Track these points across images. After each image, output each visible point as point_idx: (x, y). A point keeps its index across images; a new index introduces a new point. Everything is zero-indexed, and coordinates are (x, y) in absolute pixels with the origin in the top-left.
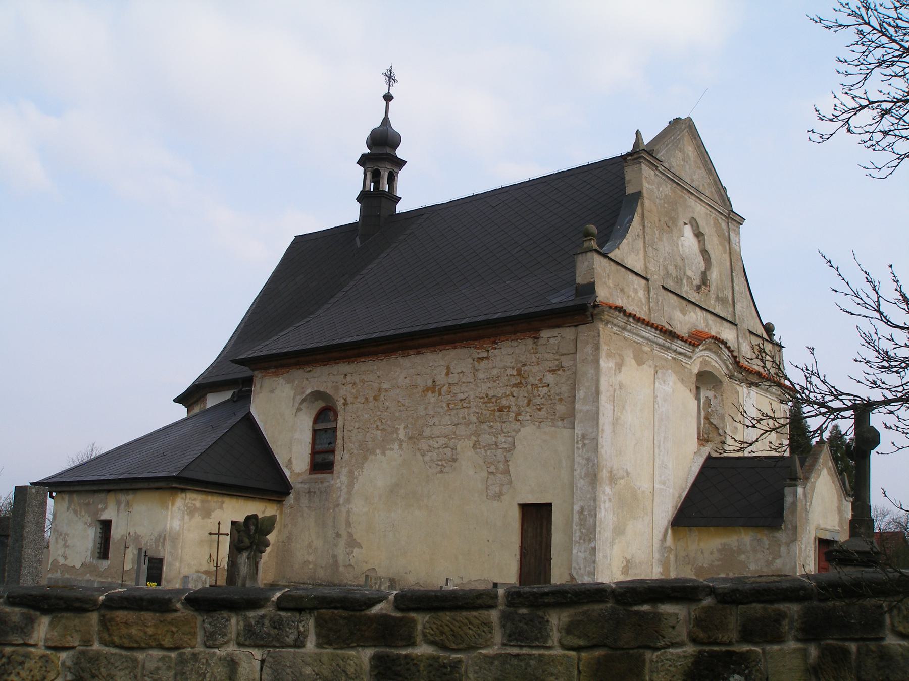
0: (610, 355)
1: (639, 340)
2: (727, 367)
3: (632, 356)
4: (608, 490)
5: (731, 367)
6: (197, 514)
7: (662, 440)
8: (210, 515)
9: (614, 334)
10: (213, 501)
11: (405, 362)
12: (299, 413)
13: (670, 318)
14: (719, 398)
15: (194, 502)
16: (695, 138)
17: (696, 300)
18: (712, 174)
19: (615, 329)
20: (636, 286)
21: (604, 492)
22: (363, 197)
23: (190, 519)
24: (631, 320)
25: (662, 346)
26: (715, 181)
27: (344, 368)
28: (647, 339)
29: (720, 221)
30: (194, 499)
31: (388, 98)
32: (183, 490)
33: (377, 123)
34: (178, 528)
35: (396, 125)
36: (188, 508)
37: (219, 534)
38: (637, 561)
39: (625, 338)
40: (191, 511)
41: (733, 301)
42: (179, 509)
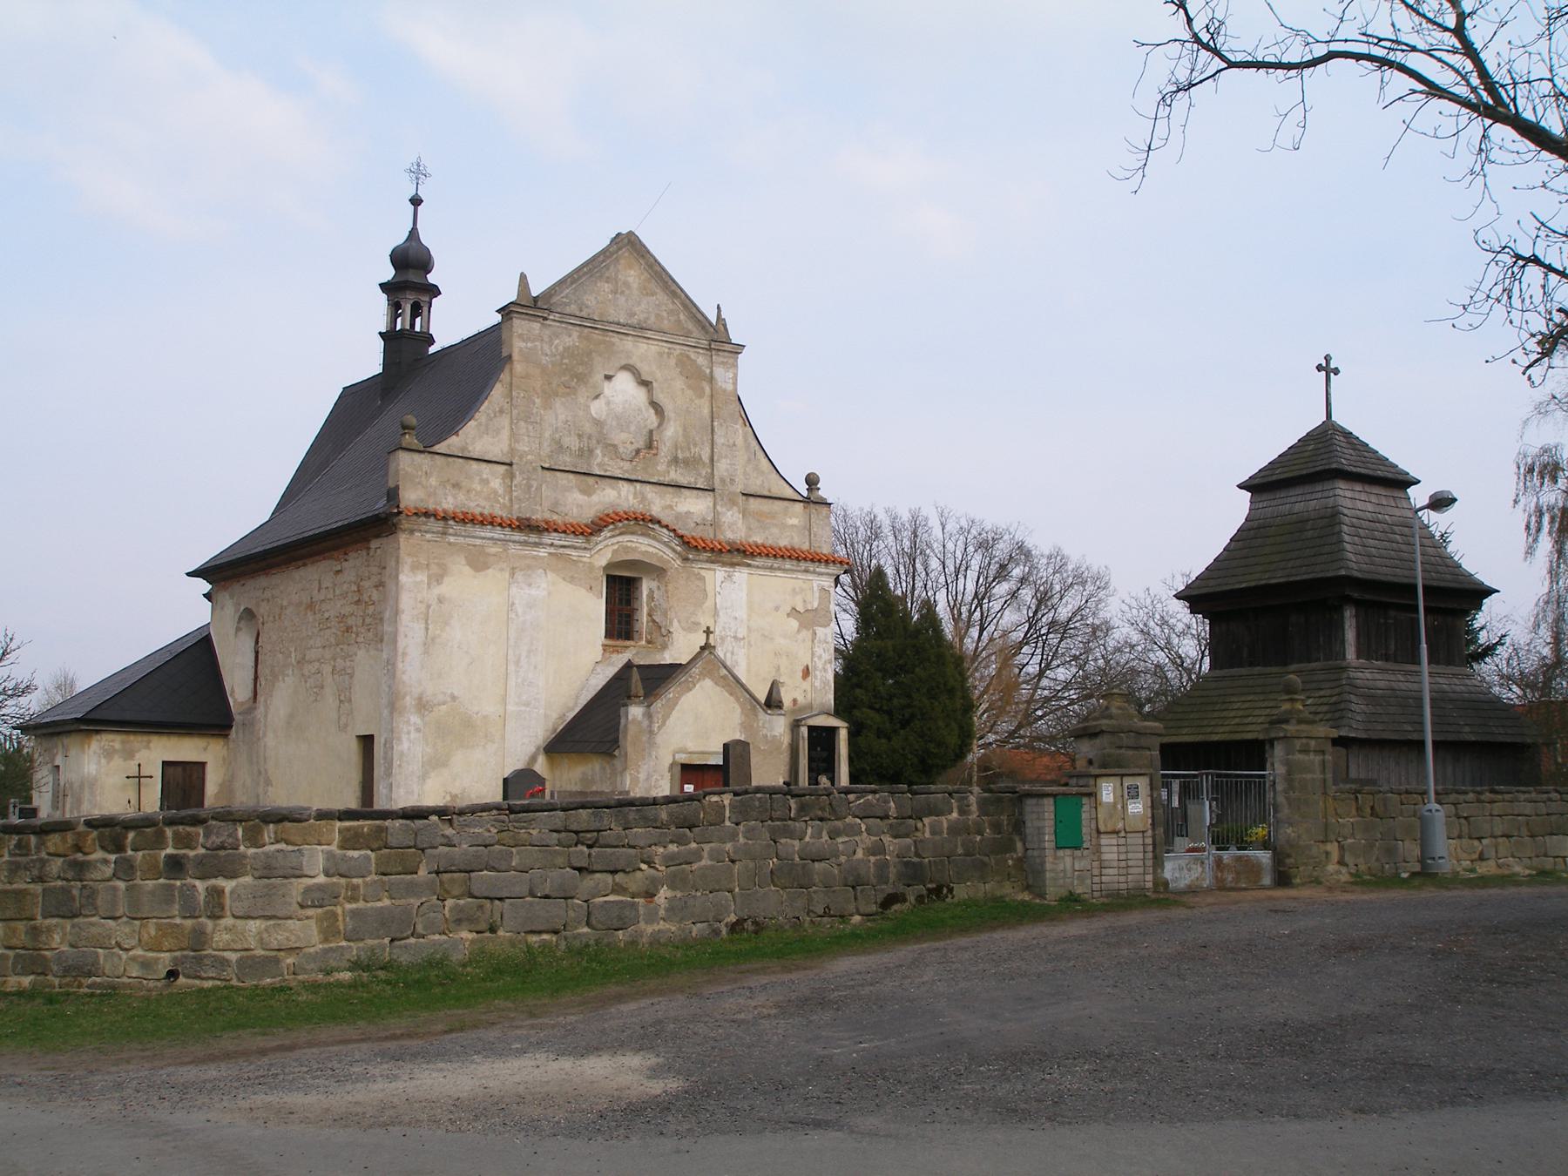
0: (415, 568)
1: (478, 542)
2: (674, 550)
3: (464, 562)
4: (415, 719)
5: (679, 549)
6: (116, 757)
7: (524, 654)
8: (134, 756)
9: (429, 541)
10: (136, 741)
11: (302, 572)
12: (240, 633)
13: (556, 503)
14: (663, 589)
16: (643, 256)
17: (627, 471)
18: (679, 297)
19: (428, 536)
20: (485, 476)
21: (408, 722)
22: (389, 337)
23: (108, 763)
24: (451, 522)
25: (525, 543)
26: (685, 306)
27: (263, 581)
28: (491, 539)
29: (693, 356)
30: (113, 741)
31: (416, 202)
32: (98, 732)
33: (400, 238)
34: (94, 772)
35: (426, 239)
36: (104, 750)
37: (139, 777)
39: (450, 544)
40: (109, 754)
41: (712, 460)
42: (95, 753)
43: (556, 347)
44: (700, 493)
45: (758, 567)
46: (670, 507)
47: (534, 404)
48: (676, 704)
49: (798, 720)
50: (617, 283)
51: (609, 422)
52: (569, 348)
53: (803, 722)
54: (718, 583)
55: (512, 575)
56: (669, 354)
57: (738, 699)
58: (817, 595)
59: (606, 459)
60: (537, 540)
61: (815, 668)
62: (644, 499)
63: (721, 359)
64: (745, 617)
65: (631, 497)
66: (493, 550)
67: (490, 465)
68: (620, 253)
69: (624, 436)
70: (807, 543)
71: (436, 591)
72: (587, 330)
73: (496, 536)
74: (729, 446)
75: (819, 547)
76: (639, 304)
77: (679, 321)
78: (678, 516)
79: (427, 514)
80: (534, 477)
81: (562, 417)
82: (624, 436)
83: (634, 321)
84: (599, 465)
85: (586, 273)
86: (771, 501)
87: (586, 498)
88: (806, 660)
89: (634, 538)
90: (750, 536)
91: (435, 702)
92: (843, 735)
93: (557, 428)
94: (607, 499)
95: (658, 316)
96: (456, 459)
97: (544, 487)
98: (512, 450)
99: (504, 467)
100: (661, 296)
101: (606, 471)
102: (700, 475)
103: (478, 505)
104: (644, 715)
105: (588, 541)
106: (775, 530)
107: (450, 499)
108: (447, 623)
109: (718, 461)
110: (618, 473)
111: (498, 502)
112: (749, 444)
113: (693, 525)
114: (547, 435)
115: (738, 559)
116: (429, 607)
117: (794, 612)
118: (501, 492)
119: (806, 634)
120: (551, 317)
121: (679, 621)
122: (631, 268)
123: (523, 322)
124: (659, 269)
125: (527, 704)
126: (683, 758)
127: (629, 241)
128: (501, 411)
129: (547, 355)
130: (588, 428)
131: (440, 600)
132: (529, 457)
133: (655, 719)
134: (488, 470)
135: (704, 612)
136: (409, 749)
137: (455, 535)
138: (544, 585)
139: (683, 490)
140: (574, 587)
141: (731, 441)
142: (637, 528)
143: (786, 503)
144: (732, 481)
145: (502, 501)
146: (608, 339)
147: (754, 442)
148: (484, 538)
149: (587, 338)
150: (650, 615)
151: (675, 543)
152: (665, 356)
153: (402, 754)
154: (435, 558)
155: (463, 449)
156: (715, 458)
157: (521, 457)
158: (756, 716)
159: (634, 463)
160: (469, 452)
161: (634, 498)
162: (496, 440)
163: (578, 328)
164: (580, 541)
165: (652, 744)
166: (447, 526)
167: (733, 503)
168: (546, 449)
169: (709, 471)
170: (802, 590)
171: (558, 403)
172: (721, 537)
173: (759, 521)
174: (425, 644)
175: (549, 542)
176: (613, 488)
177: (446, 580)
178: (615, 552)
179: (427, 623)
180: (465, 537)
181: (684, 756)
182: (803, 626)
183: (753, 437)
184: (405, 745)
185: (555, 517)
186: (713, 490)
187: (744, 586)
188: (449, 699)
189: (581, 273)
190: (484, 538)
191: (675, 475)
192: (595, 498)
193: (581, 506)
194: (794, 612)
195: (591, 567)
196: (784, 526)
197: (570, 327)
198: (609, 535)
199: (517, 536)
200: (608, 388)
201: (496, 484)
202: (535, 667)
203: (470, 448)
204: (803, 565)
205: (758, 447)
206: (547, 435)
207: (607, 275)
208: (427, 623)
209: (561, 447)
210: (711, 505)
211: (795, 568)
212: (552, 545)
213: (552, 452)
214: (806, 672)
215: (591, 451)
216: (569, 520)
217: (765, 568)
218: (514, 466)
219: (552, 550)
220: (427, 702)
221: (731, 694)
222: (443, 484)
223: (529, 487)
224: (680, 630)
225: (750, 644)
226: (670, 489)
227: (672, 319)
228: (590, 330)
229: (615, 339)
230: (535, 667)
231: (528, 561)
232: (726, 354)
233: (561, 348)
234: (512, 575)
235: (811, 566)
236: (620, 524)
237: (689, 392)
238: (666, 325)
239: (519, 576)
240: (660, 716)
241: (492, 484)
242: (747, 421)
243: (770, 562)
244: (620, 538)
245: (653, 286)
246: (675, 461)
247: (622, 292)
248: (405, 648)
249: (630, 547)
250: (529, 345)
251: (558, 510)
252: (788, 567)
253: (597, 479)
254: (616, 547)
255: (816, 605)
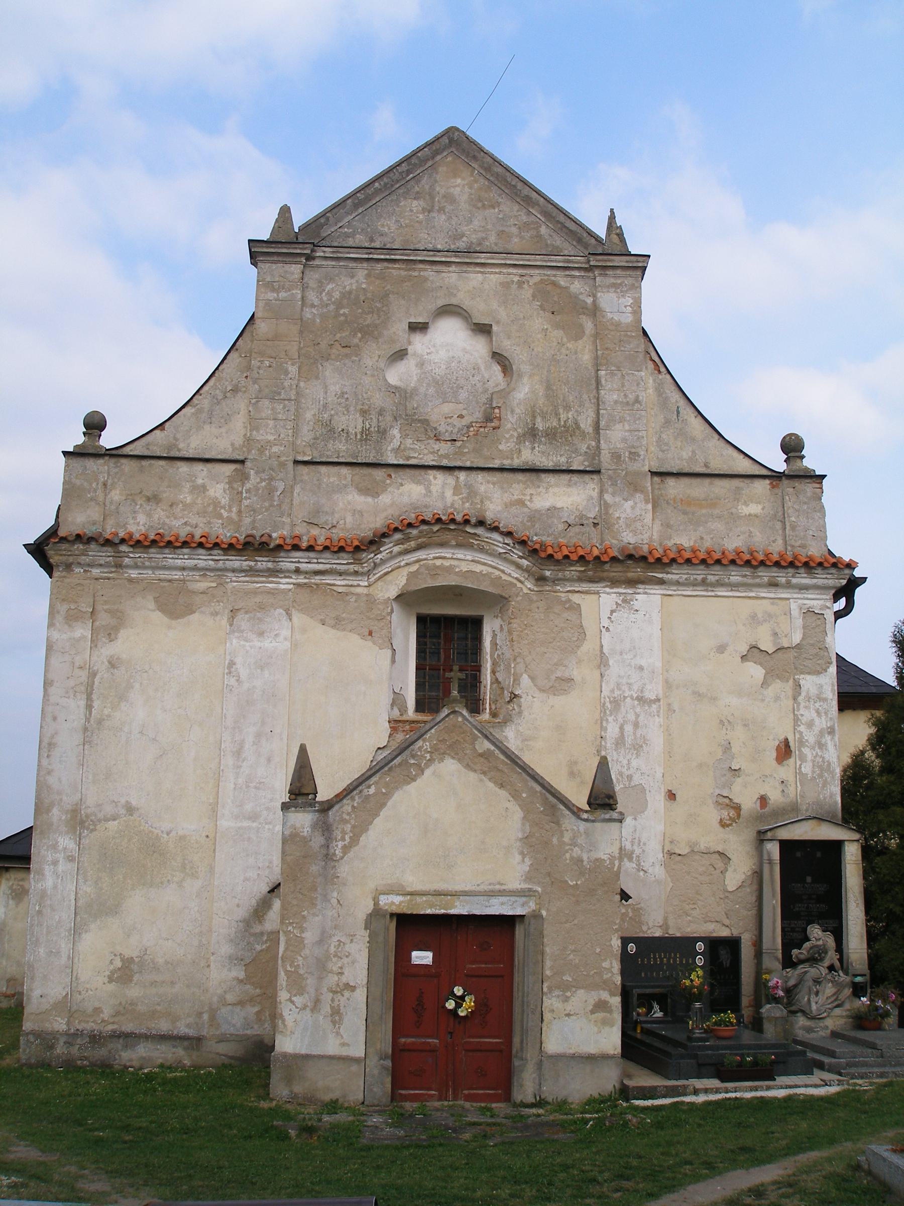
1: (177, 575)
2: (518, 566)
3: (152, 605)
4: (66, 842)
5: (525, 563)
7: (250, 739)
13: (317, 511)
15: (21, 883)
16: (475, 158)
17: (446, 456)
18: (535, 204)
19: (96, 572)
20: (200, 481)
21: (54, 847)
23: (17, 906)
26: (546, 214)
28: (195, 568)
29: (563, 282)
36: (13, 891)
38: (161, 961)
39: (131, 580)
41: (597, 427)
42: (4, 894)
43: (329, 294)
44: (575, 478)
45: (678, 583)
46: (521, 503)
47: (287, 373)
48: (383, 805)
49: (760, 833)
50: (432, 198)
51: (422, 390)
52: (350, 292)
53: (769, 835)
54: (605, 614)
55: (232, 618)
56: (520, 284)
57: (515, 795)
58: (799, 622)
59: (409, 442)
60: (270, 565)
61: (802, 743)
62: (472, 493)
63: (612, 280)
64: (659, 664)
65: (449, 493)
66: (203, 585)
67: (210, 466)
68: (439, 157)
69: (447, 408)
70: (780, 541)
71: (107, 650)
72: (379, 266)
73: (202, 564)
74: (627, 404)
75: (803, 546)
76: (470, 221)
77: (539, 236)
78: (534, 517)
79: (90, 540)
80: (281, 475)
81: (334, 388)
82: (447, 408)
83: (461, 244)
84: (397, 451)
85: (377, 192)
86: (707, 481)
87: (370, 499)
88: (783, 730)
89: (446, 552)
90: (670, 538)
91: (100, 815)
92: (852, 854)
93: (325, 406)
94: (406, 499)
95: (501, 234)
96: (153, 462)
97: (297, 489)
98: (248, 440)
99: (232, 467)
100: (509, 207)
101: (408, 458)
102: (576, 451)
103: (186, 523)
104: (314, 826)
105: (358, 561)
106: (718, 526)
107: (142, 518)
108: (122, 698)
109: (608, 428)
110: (429, 460)
111: (220, 516)
112: (667, 398)
113: (561, 527)
114: (309, 415)
115: (637, 571)
116: (93, 675)
117: (754, 652)
118: (225, 501)
119: (777, 687)
120: (319, 254)
121: (532, 678)
122: (455, 176)
123: (274, 266)
124: (499, 170)
125: (254, 817)
126: (395, 902)
127: (451, 141)
128: (235, 390)
129: (313, 306)
130: (378, 399)
131: (113, 664)
132: (275, 449)
133: (338, 834)
134: (205, 473)
135: (580, 662)
136: (55, 887)
137: (136, 567)
138: (286, 632)
139: (543, 476)
140: (340, 633)
141: (631, 397)
142: (447, 536)
143: (736, 482)
144: (634, 456)
145: (225, 514)
146: (416, 274)
147: (675, 396)
148: (184, 569)
149: (382, 277)
150: (493, 672)
151: (517, 553)
152: (515, 286)
153: (43, 895)
154: (106, 602)
155: (170, 448)
156: (602, 423)
157: (261, 450)
158: (558, 823)
159: (458, 444)
160: (179, 450)
161: (454, 494)
162: (223, 430)
163: (365, 265)
164: (342, 562)
165: (330, 878)
166: (119, 555)
167: (633, 486)
168: (306, 434)
169: (593, 443)
170: (769, 616)
171: (328, 371)
172: (610, 541)
173: (685, 513)
174: (85, 729)
175: (293, 566)
176: (418, 483)
177: (123, 633)
178: (412, 576)
179: (89, 698)
180: (153, 568)
181: (397, 899)
182: (772, 674)
183: (673, 387)
184: (49, 882)
185: (315, 531)
186: (598, 472)
187: (656, 617)
188: (123, 811)
189: (370, 191)
190: (184, 569)
191: (528, 456)
192: (385, 499)
193: (361, 513)
194: (754, 652)
195: (371, 601)
196: (734, 518)
197: (352, 264)
198: (396, 549)
199: (236, 562)
200: (419, 344)
201: (218, 491)
202: (269, 760)
203: (181, 446)
204: (765, 575)
205: (682, 402)
206: (309, 415)
207: (417, 189)
208: (89, 698)
209: (332, 430)
210: (595, 494)
211: (750, 581)
212: (297, 571)
213: (316, 438)
214: (785, 751)
215: (383, 433)
216: (337, 534)
217: (694, 584)
218: (248, 464)
219: (302, 580)
220: (87, 816)
221: (502, 786)
222: (131, 497)
223: (271, 491)
224: (537, 694)
225: (670, 709)
226: (520, 477)
227: (527, 235)
228: (386, 264)
229: (429, 273)
230: (269, 760)
231: (258, 599)
232: (619, 272)
233: (337, 295)
234: (232, 618)
235: (782, 577)
236: (414, 532)
237: (558, 334)
238: (515, 244)
239: (242, 620)
240: (348, 827)
241: (211, 493)
242: (659, 365)
243: (699, 573)
244: (421, 554)
245: (494, 194)
246: (532, 434)
247: (442, 210)
248: (53, 737)
249: (441, 568)
250: (283, 295)
251: (322, 519)
252: (735, 579)
253: (390, 471)
254: (414, 568)
255: (797, 638)
